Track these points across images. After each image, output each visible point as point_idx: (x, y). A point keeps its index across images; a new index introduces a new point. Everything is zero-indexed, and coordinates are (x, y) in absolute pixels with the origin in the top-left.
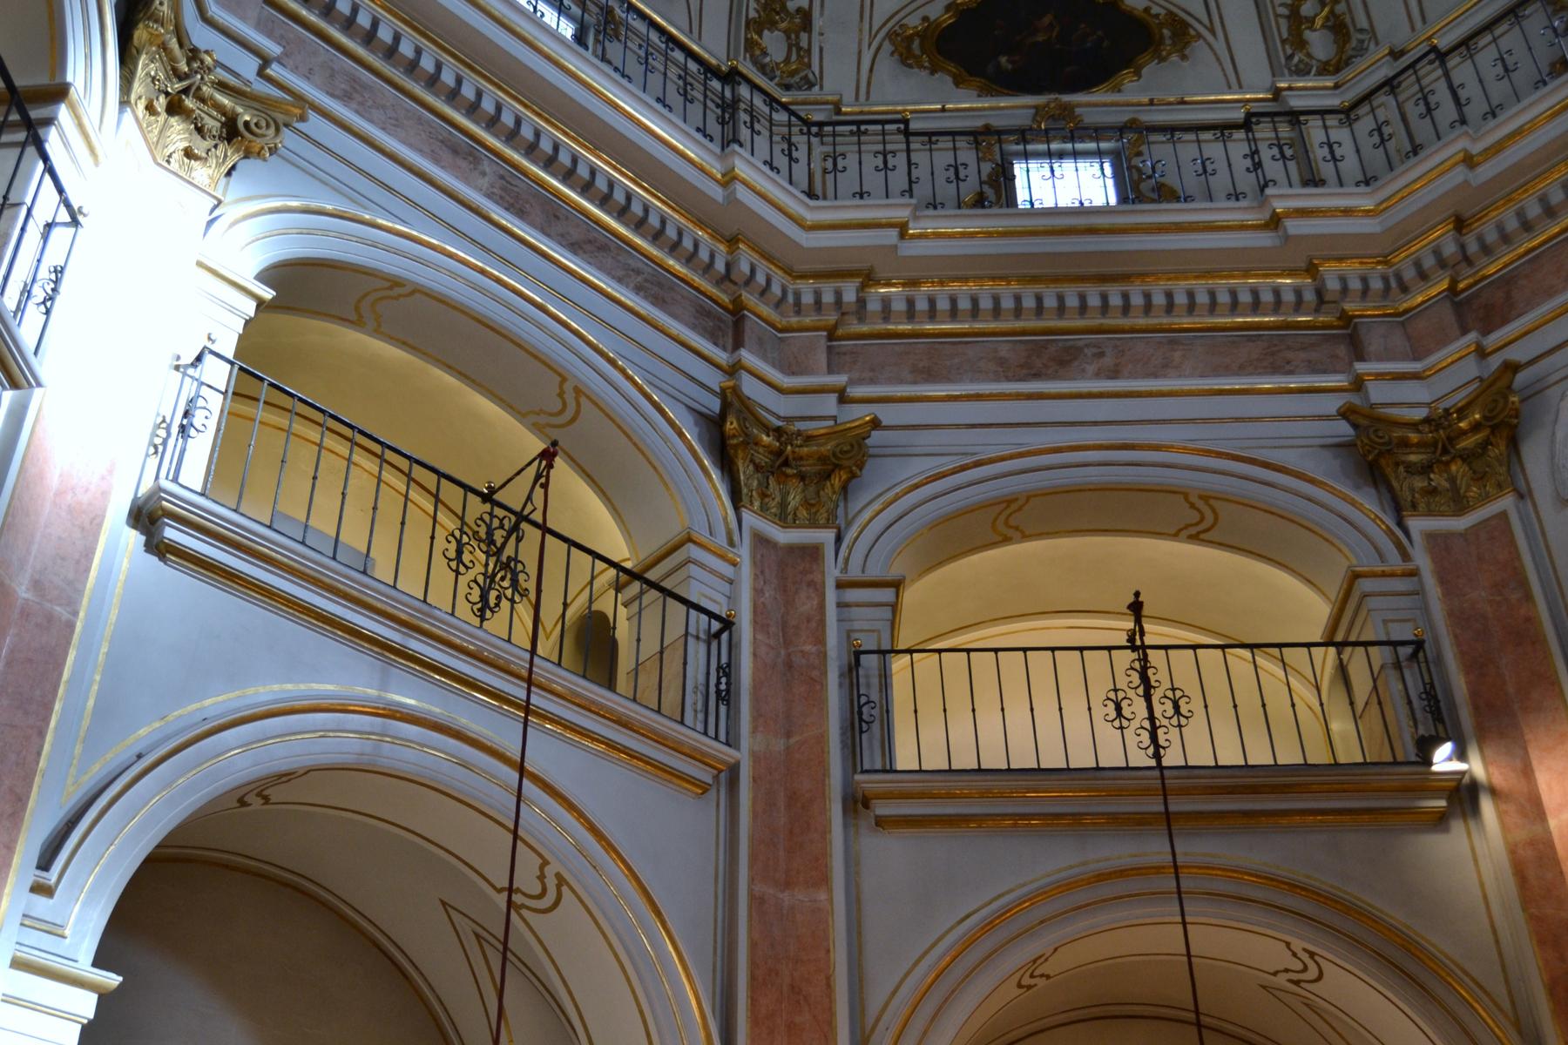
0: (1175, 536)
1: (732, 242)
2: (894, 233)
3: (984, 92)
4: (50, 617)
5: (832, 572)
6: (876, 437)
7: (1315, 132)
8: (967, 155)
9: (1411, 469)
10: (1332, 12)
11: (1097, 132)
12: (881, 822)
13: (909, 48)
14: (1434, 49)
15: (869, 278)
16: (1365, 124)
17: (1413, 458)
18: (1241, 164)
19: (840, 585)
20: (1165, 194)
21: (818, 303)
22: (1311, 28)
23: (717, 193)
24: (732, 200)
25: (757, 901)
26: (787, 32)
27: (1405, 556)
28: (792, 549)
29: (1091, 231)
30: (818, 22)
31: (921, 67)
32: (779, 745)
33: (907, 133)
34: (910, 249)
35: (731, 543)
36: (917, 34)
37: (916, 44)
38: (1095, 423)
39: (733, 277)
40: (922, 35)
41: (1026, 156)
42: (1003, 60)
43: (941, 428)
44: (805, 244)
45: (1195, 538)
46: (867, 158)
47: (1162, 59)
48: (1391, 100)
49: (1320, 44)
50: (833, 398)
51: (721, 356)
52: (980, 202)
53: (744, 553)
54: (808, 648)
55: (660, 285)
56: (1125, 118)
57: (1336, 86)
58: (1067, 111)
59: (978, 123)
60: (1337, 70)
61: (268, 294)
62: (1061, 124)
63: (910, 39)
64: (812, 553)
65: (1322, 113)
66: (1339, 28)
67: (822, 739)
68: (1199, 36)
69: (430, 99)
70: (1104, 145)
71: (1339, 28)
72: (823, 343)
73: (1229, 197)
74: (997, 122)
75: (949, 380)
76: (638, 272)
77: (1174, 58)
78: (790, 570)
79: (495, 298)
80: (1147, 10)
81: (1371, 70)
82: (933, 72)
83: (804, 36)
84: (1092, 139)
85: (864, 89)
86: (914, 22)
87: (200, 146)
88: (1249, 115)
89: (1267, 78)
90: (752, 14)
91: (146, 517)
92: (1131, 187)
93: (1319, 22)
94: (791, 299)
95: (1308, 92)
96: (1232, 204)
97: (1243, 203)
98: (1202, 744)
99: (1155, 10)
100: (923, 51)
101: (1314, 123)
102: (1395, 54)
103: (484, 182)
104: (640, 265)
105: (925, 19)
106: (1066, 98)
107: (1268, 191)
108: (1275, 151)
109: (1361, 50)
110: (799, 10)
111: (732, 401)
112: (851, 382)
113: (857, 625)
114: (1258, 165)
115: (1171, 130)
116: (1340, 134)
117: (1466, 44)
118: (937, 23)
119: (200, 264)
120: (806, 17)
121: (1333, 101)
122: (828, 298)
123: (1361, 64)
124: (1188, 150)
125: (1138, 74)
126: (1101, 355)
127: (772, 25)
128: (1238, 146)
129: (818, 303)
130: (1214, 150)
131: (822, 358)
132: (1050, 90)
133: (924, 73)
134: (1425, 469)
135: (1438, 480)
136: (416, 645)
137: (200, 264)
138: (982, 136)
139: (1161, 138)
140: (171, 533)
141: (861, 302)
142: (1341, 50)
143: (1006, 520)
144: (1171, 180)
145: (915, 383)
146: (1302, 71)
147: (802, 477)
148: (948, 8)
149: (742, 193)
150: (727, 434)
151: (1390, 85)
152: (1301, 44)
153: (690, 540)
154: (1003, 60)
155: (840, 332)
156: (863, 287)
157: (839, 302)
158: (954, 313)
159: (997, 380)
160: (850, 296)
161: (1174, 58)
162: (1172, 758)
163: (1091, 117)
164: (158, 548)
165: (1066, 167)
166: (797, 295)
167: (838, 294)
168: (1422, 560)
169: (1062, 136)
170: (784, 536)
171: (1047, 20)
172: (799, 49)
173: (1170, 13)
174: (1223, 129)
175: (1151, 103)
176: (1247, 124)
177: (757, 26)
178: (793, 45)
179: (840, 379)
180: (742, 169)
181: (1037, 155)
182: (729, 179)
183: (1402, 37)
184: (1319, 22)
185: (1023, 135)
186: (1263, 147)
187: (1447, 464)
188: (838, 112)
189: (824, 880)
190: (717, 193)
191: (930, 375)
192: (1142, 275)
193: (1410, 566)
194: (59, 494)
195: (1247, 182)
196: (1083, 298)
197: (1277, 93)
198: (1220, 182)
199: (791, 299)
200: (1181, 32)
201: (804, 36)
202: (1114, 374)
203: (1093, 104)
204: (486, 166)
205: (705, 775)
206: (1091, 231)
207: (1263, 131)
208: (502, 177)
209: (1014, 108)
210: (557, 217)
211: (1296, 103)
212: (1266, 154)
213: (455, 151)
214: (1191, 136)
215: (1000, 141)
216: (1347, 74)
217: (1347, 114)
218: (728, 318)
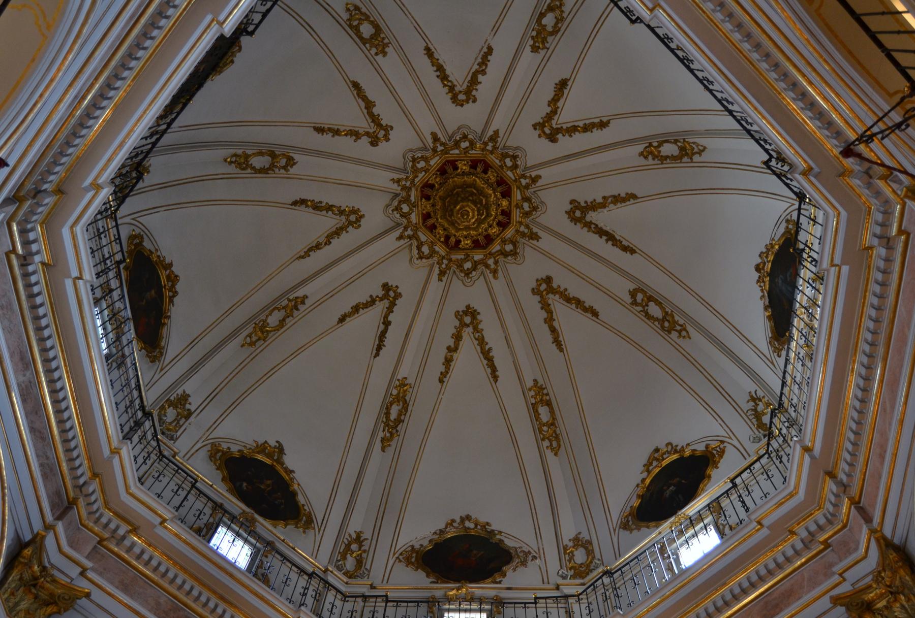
1: (95, 475)
2: (159, 520)
3: (230, 491)
6: (84, 601)
7: (330, 596)
8: (208, 511)
10: (361, 554)
11: (259, 538)
13: (216, 453)
14: (386, 596)
15: (135, 530)
16: (349, 606)
18: (299, 590)
20: (265, 580)
21: (106, 526)
22: (351, 555)
23: (106, 452)
24: (110, 460)
26: (178, 414)
29: (231, 576)
30: (192, 419)
31: (215, 464)
33: (193, 486)
34: (160, 531)
36: (223, 451)
37: (220, 454)
39: (83, 489)
40: (224, 453)
41: (229, 528)
42: (245, 484)
46: (172, 484)
47: (296, 527)
48: (362, 604)
49: (350, 563)
50: (80, 570)
51: (49, 518)
52: (198, 531)
55: (51, 470)
56: (271, 539)
57: (347, 583)
58: (253, 521)
59: (219, 500)
60: (350, 577)
62: (248, 524)
63: (219, 451)
65: (338, 591)
66: (359, 562)
68: (314, 528)
69: (32, 333)
70: (258, 544)
71: (359, 562)
72: (94, 543)
73: (287, 599)
74: (227, 506)
75: (131, 597)
76: (47, 458)
77: (301, 530)
80: (303, 505)
81: (360, 587)
82: (217, 469)
83: (183, 420)
84: (255, 539)
85: (189, 455)
86: (224, 446)
88: (314, 572)
89: (326, 562)
90: (172, 398)
92: (257, 568)
93: (354, 555)
94: (97, 515)
95: (336, 579)
96: (287, 603)
97: (291, 606)
99: (306, 508)
100: (220, 459)
101: (333, 592)
102: (372, 587)
103: (22, 378)
104: (51, 456)
105: (229, 448)
106: (256, 516)
107: (302, 608)
108: (314, 593)
109: (362, 577)
110: (189, 410)
111: (37, 542)
112: (93, 569)
114: (304, 594)
115: (285, 558)
116: (338, 603)
117: (397, 602)
118: (232, 453)
120: (189, 414)
121: (343, 588)
122: (112, 526)
123: (359, 581)
124: (285, 570)
125: (286, 526)
127: (176, 407)
128: (303, 582)
129: (106, 526)
130: (294, 576)
131: (89, 548)
132: (253, 508)
133: (215, 467)
138: (217, 507)
139: (279, 557)
141: (124, 538)
142: (356, 570)
144: (272, 577)
145: (117, 588)
146: (339, 568)
148: (239, 451)
149: (116, 461)
151: (365, 598)
152: (344, 558)
154: (245, 484)
158: (155, 569)
160: (121, 532)
161: (301, 530)
163: (259, 530)
165: (239, 543)
166: (101, 515)
167: (118, 527)
169: (244, 529)
171: (269, 482)
172: (178, 423)
173: (310, 513)
174: (302, 571)
175: (283, 541)
176: (311, 575)
177: (171, 403)
178: (177, 420)
179: (88, 564)
180: (124, 452)
181: (233, 530)
182: (115, 452)
183: (377, 582)
184: (354, 555)
185: (233, 518)
186: (311, 588)
188: (174, 457)
190: (106, 452)
191: (125, 589)
192: (236, 607)
195: (297, 597)
196: (208, 600)
197: (326, 570)
198: (288, 590)
199: (97, 515)
200: (309, 522)
201: (183, 420)
203: (264, 525)
204: (28, 373)
206: (231, 576)
207: (315, 582)
208: (30, 382)
209: (236, 505)
210: (36, 413)
211: (331, 579)
212: (311, 592)
213: (22, 358)
214: (290, 565)
215: (223, 515)
216: (350, 581)
217: (345, 597)
218: (66, 503)
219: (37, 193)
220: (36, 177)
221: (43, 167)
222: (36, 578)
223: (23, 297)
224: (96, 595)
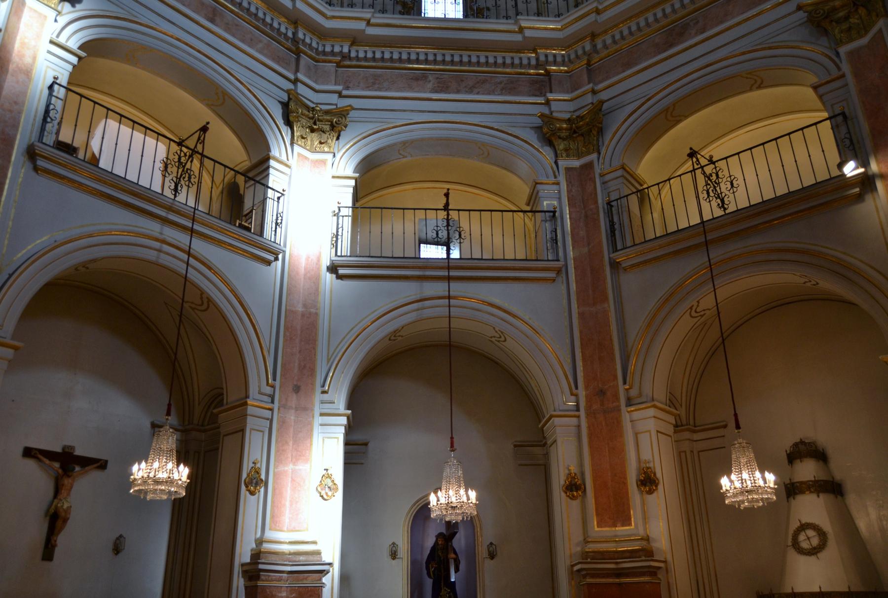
0: (751, 90)
1: (534, 51)
4: (310, 314)
5: (597, 170)
9: (838, 22)
12: (625, 269)
15: (593, 36)
17: (841, 14)
19: (601, 175)
23: (518, 38)
24: (524, 37)
25: (581, 315)
27: (839, 69)
28: (583, 167)
32: (585, 250)
35: (555, 177)
38: (696, 59)
43: (632, 89)
44: (562, 37)
45: (759, 87)
50: (590, 95)
51: (541, 100)
53: (562, 179)
54: (592, 206)
61: (357, 175)
64: (589, 166)
67: (600, 243)
75: (637, 64)
76: (501, 83)
78: (581, 178)
79: (441, 129)
87: (325, 136)
91: (333, 269)
94: (566, 59)
98: (739, 200)
103: (430, 85)
111: (548, 119)
113: (611, 189)
119: (333, 177)
126: (697, 22)
131: (585, 77)
134: (847, 18)
135: (854, 20)
136: (429, 273)
137: (333, 177)
140: (341, 271)
143: (671, 116)
145: (624, 71)
147: (582, 135)
149: (528, 33)
150: (549, 133)
153: (537, 183)
155: (593, 62)
156: (593, 40)
157: (584, 53)
159: (655, 56)
160: (588, 47)
162: (732, 208)
164: (340, 277)
168: (846, 68)
170: (576, 163)
179: (591, 85)
180: (524, 24)
182: (521, 30)
187: (856, 10)
189: (606, 299)
191: (628, 65)
193: (841, 73)
194: (305, 275)
199: (566, 59)
202: (703, 31)
204: (430, 78)
205: (552, 275)
213: (417, 79)
219: (295, 40)
220: (282, 39)
221: (275, 34)
222: (571, 129)
223: (374, 64)
224: (604, 96)
